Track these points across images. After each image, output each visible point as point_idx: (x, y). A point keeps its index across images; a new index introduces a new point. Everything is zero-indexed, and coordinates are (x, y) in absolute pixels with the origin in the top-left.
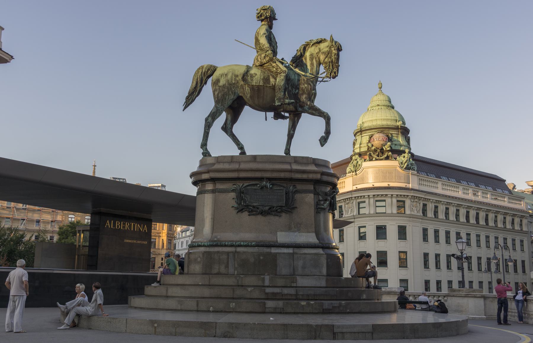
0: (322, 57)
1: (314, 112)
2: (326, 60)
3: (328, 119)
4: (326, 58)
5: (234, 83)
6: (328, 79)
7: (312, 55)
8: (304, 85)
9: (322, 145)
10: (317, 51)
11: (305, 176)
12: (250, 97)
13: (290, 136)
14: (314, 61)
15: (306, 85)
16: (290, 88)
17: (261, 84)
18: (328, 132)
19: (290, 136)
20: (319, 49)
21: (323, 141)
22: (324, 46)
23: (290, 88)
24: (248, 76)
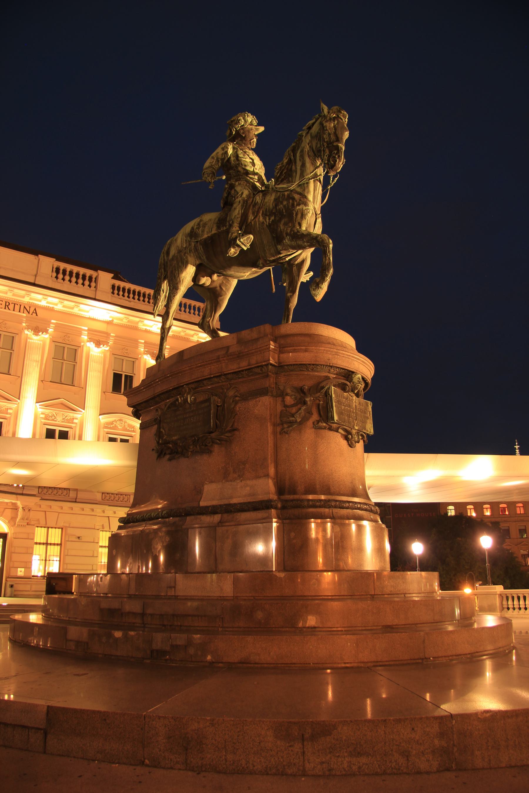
1: (300, 242)
4: (317, 143)
5: (186, 247)
10: (308, 141)
12: (206, 258)
15: (285, 203)
16: (261, 219)
17: (214, 231)
24: (198, 228)
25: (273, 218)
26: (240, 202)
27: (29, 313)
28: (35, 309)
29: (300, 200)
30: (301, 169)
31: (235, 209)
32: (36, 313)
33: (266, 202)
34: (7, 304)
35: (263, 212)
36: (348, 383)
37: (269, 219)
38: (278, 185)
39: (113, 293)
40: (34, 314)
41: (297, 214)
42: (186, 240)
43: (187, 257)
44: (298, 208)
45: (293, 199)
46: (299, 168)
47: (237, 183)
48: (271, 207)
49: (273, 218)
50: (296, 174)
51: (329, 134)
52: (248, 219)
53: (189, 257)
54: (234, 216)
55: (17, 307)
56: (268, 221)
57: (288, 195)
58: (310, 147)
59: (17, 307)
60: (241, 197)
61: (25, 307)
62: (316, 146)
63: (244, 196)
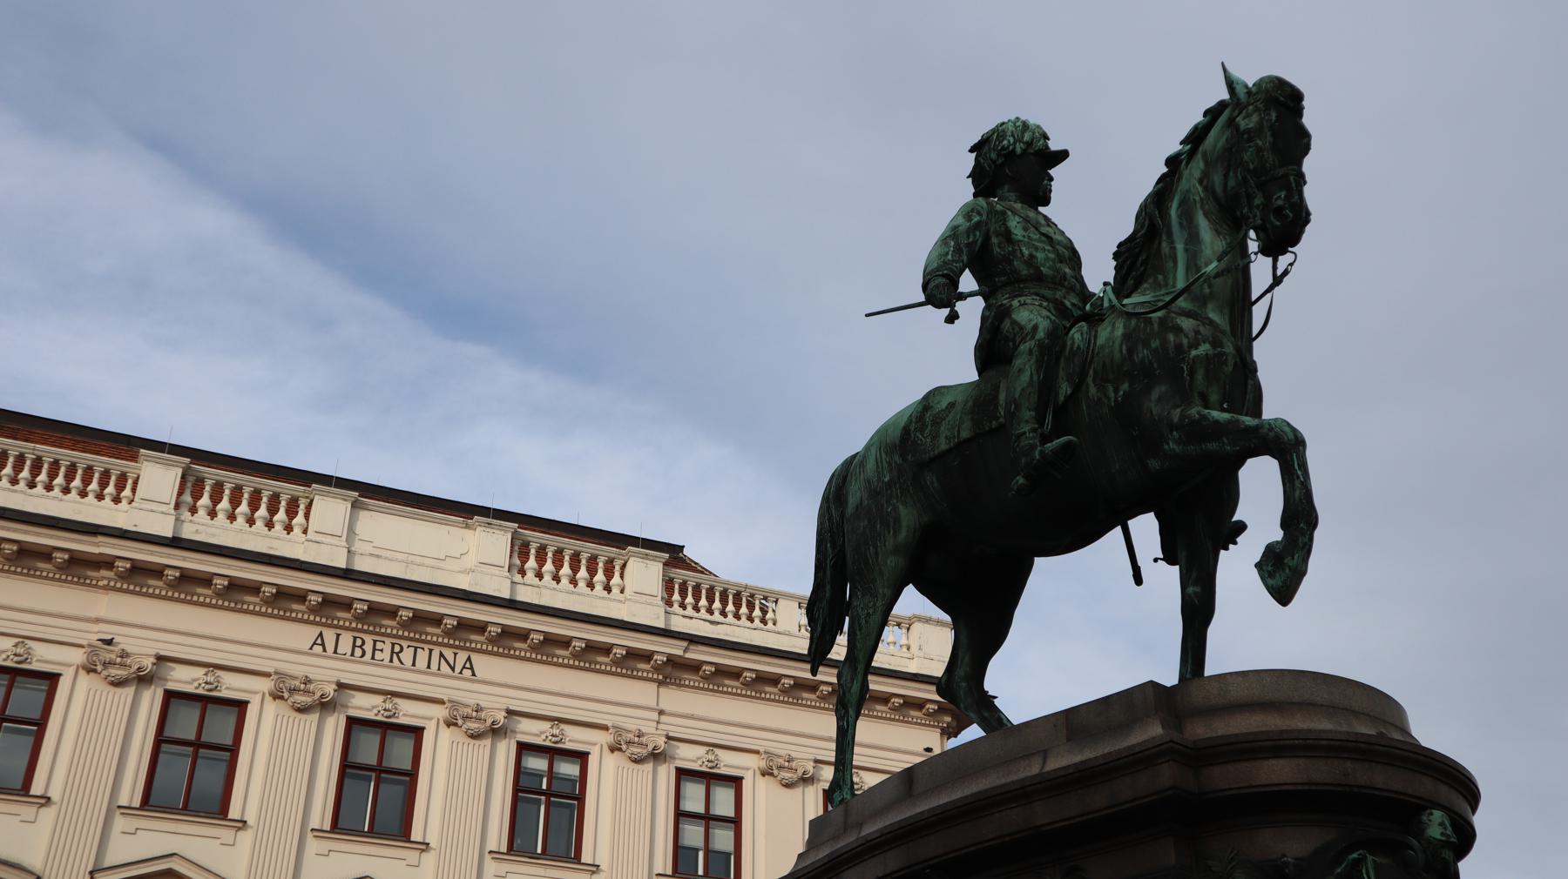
0: (1217, 179)
2: (1232, 183)
3: (1287, 447)
4: (1226, 176)
6: (1284, 261)
7: (1184, 203)
8: (1146, 344)
9: (1283, 595)
10: (1197, 174)
11: (1097, 799)
13: (1198, 610)
14: (1203, 223)
15: (1155, 344)
16: (1093, 390)
17: (965, 434)
18: (1300, 516)
19: (1198, 610)
20: (1204, 155)
21: (1283, 571)
22: (1213, 139)
23: (1093, 390)
25: (1126, 386)
26: (1030, 351)
27: (453, 669)
28: (469, 659)
29: (1197, 332)
30: (1186, 250)
31: (1020, 371)
32: (472, 668)
33: (1102, 346)
34: (397, 649)
35: (1095, 372)
36: (1415, 842)
37: (1116, 390)
38: (1128, 296)
39: (669, 603)
40: (467, 673)
41: (1192, 372)
42: (889, 464)
43: (895, 509)
44: (1194, 353)
45: (1178, 330)
46: (1180, 247)
47: (1015, 303)
48: (1117, 355)
49: (1126, 386)
50: (1175, 262)
51: (1259, 150)
52: (1057, 394)
53: (901, 508)
54: (1019, 389)
55: (422, 657)
56: (1112, 395)
57: (1162, 321)
58: (1205, 189)
59: (422, 657)
60: (1033, 338)
61: (441, 655)
62: (1225, 185)
63: (1041, 334)
